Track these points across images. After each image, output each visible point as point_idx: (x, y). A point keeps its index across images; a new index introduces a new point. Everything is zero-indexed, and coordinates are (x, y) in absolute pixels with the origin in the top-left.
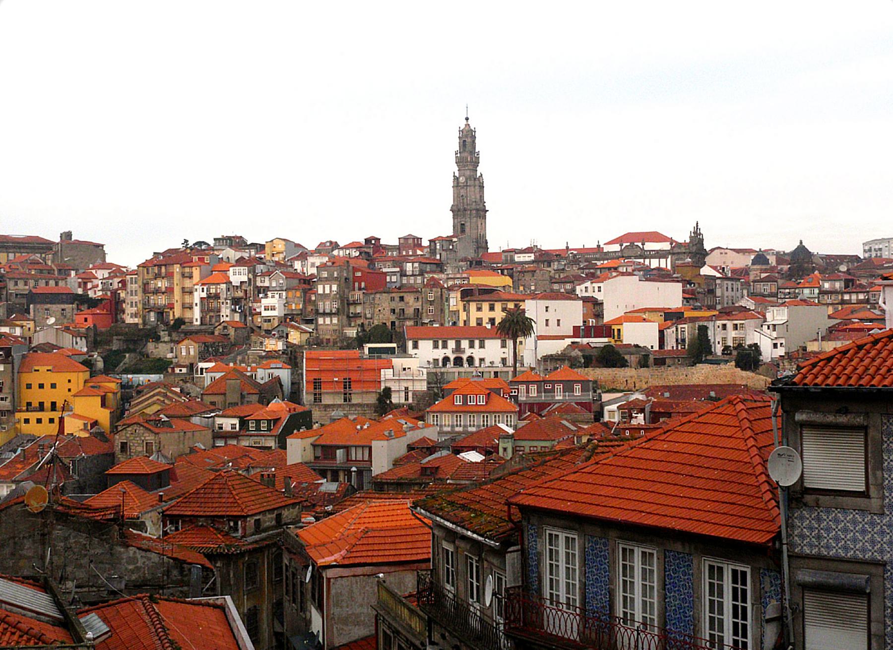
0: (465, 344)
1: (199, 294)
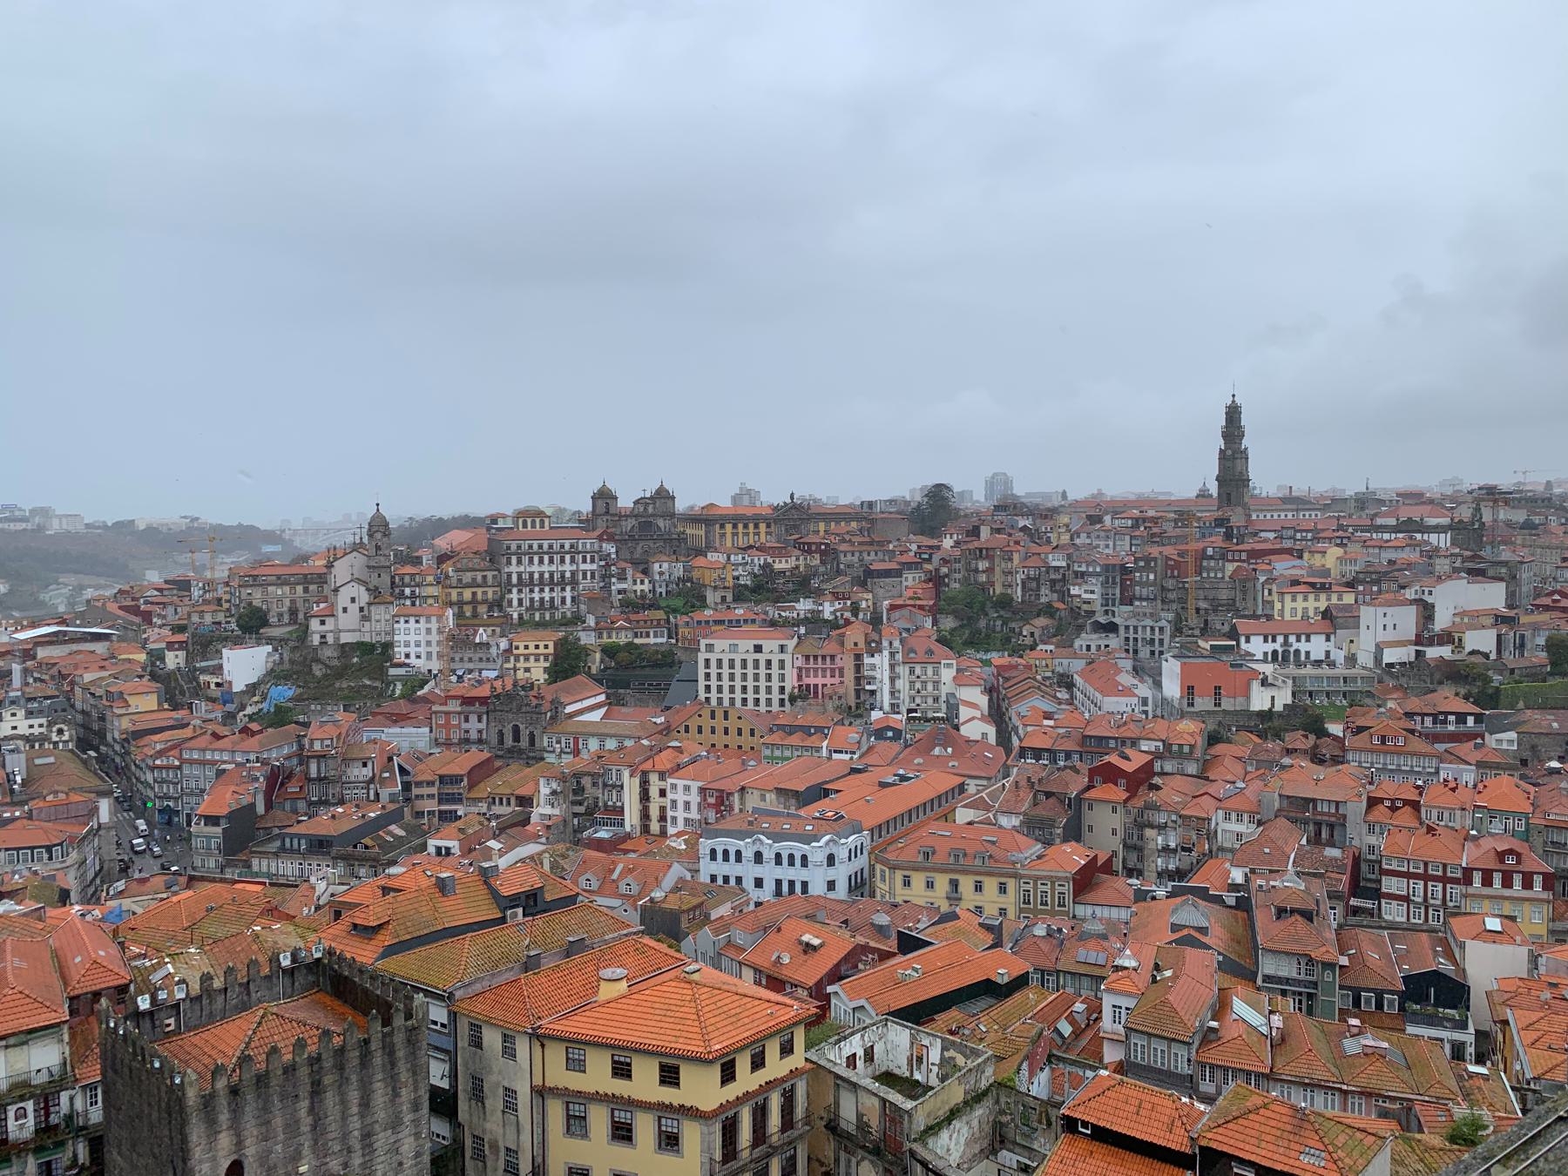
0: (1292, 639)
1: (1019, 577)
